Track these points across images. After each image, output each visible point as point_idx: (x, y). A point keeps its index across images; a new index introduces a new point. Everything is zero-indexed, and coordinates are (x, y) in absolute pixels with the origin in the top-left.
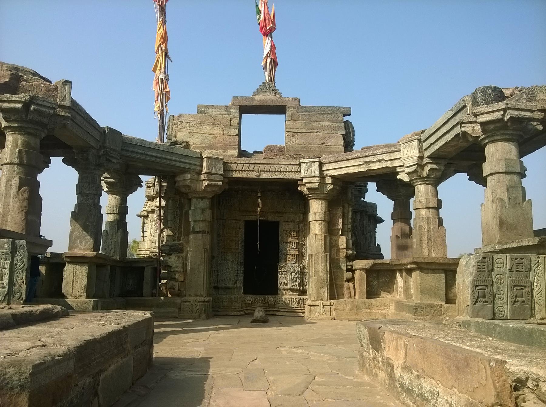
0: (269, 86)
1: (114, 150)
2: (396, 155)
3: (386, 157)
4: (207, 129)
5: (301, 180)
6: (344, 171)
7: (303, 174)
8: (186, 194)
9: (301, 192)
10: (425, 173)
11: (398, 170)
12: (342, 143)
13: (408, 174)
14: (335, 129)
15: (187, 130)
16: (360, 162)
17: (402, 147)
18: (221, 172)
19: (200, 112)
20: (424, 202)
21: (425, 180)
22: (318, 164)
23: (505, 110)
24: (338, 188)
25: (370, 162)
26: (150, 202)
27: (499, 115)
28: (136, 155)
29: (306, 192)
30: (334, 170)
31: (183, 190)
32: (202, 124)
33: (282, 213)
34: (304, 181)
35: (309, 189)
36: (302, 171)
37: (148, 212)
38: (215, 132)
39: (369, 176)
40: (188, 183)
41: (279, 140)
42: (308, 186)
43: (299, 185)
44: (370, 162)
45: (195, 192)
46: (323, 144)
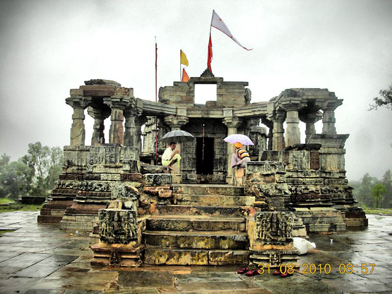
0: (208, 71)
1: (140, 108)
2: (265, 109)
3: (261, 109)
4: (179, 93)
5: (224, 118)
6: (243, 115)
7: (224, 116)
8: (169, 125)
9: (224, 124)
10: (277, 117)
11: (267, 115)
12: (244, 100)
13: (270, 117)
14: (240, 93)
15: (169, 94)
16: (250, 111)
17: (268, 105)
18: (186, 115)
19: (175, 85)
20: (276, 130)
21: (277, 120)
22: (232, 111)
23: (290, 101)
24: (241, 122)
25: (255, 111)
26: (147, 128)
27: (288, 102)
28: (166, 112)
29: (226, 124)
30: (240, 114)
31: (168, 123)
32: (176, 91)
33: (199, 133)
34: (225, 119)
35: (227, 123)
36: (224, 114)
37: (147, 133)
38: (182, 95)
39: (256, 117)
40: (170, 120)
41: (214, 98)
42: (227, 121)
43: (222, 121)
44: (255, 111)
45: (173, 124)
46: (235, 100)
